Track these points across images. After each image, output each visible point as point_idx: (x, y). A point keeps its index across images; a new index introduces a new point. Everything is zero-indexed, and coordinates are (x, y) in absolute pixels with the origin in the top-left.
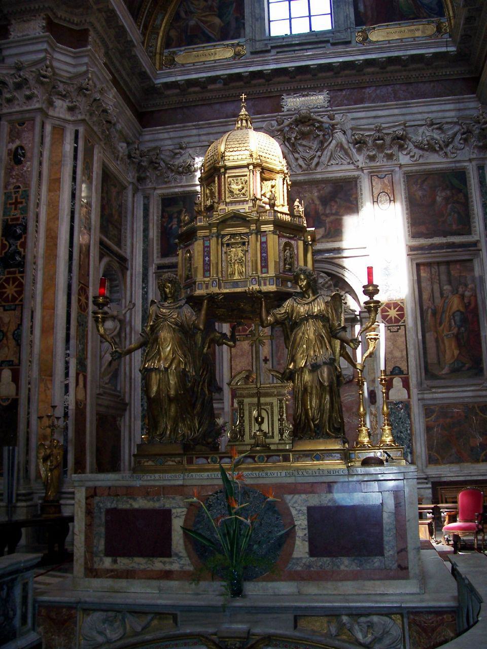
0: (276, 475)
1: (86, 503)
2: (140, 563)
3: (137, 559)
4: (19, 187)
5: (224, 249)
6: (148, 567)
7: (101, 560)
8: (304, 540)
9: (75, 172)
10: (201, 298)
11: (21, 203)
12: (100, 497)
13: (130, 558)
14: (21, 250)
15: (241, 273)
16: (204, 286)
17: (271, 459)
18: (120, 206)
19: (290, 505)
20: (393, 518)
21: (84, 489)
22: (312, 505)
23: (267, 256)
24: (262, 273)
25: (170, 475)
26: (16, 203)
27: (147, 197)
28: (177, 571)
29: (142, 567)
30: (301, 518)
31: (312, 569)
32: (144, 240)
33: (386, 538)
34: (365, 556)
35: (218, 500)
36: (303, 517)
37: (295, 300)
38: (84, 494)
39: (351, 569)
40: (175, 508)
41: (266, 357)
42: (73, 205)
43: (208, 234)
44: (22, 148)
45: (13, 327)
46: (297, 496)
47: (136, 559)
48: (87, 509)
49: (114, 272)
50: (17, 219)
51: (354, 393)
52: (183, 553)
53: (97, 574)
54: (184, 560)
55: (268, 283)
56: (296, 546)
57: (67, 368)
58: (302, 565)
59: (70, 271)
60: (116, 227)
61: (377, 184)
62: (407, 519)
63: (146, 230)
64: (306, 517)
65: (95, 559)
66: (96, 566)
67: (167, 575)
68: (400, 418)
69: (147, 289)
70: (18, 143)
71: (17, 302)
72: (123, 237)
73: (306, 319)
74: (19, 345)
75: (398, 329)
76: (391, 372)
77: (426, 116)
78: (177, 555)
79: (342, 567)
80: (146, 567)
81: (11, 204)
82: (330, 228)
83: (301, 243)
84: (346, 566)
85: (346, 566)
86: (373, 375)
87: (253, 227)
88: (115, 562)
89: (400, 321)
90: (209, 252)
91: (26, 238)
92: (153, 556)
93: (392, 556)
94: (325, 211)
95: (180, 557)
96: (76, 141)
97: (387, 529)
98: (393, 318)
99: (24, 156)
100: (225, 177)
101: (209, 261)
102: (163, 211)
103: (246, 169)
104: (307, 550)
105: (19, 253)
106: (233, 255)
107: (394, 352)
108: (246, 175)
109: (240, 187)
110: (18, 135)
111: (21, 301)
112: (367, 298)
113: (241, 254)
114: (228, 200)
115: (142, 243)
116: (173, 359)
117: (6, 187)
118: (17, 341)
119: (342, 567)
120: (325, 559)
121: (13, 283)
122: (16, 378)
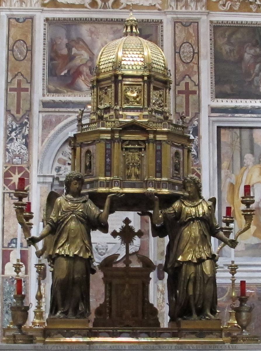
0: (167, 348)
10: (104, 195)
15: (137, 176)
16: (105, 184)
37: (183, 203)
43: (109, 138)
61: (180, 31)
73: (193, 220)
83: (186, 151)
87: (151, 136)
100: (121, 85)
103: (141, 80)
106: (130, 158)
109: (135, 95)
112: (243, 207)
113: (137, 158)
114: (125, 106)
116: (81, 248)
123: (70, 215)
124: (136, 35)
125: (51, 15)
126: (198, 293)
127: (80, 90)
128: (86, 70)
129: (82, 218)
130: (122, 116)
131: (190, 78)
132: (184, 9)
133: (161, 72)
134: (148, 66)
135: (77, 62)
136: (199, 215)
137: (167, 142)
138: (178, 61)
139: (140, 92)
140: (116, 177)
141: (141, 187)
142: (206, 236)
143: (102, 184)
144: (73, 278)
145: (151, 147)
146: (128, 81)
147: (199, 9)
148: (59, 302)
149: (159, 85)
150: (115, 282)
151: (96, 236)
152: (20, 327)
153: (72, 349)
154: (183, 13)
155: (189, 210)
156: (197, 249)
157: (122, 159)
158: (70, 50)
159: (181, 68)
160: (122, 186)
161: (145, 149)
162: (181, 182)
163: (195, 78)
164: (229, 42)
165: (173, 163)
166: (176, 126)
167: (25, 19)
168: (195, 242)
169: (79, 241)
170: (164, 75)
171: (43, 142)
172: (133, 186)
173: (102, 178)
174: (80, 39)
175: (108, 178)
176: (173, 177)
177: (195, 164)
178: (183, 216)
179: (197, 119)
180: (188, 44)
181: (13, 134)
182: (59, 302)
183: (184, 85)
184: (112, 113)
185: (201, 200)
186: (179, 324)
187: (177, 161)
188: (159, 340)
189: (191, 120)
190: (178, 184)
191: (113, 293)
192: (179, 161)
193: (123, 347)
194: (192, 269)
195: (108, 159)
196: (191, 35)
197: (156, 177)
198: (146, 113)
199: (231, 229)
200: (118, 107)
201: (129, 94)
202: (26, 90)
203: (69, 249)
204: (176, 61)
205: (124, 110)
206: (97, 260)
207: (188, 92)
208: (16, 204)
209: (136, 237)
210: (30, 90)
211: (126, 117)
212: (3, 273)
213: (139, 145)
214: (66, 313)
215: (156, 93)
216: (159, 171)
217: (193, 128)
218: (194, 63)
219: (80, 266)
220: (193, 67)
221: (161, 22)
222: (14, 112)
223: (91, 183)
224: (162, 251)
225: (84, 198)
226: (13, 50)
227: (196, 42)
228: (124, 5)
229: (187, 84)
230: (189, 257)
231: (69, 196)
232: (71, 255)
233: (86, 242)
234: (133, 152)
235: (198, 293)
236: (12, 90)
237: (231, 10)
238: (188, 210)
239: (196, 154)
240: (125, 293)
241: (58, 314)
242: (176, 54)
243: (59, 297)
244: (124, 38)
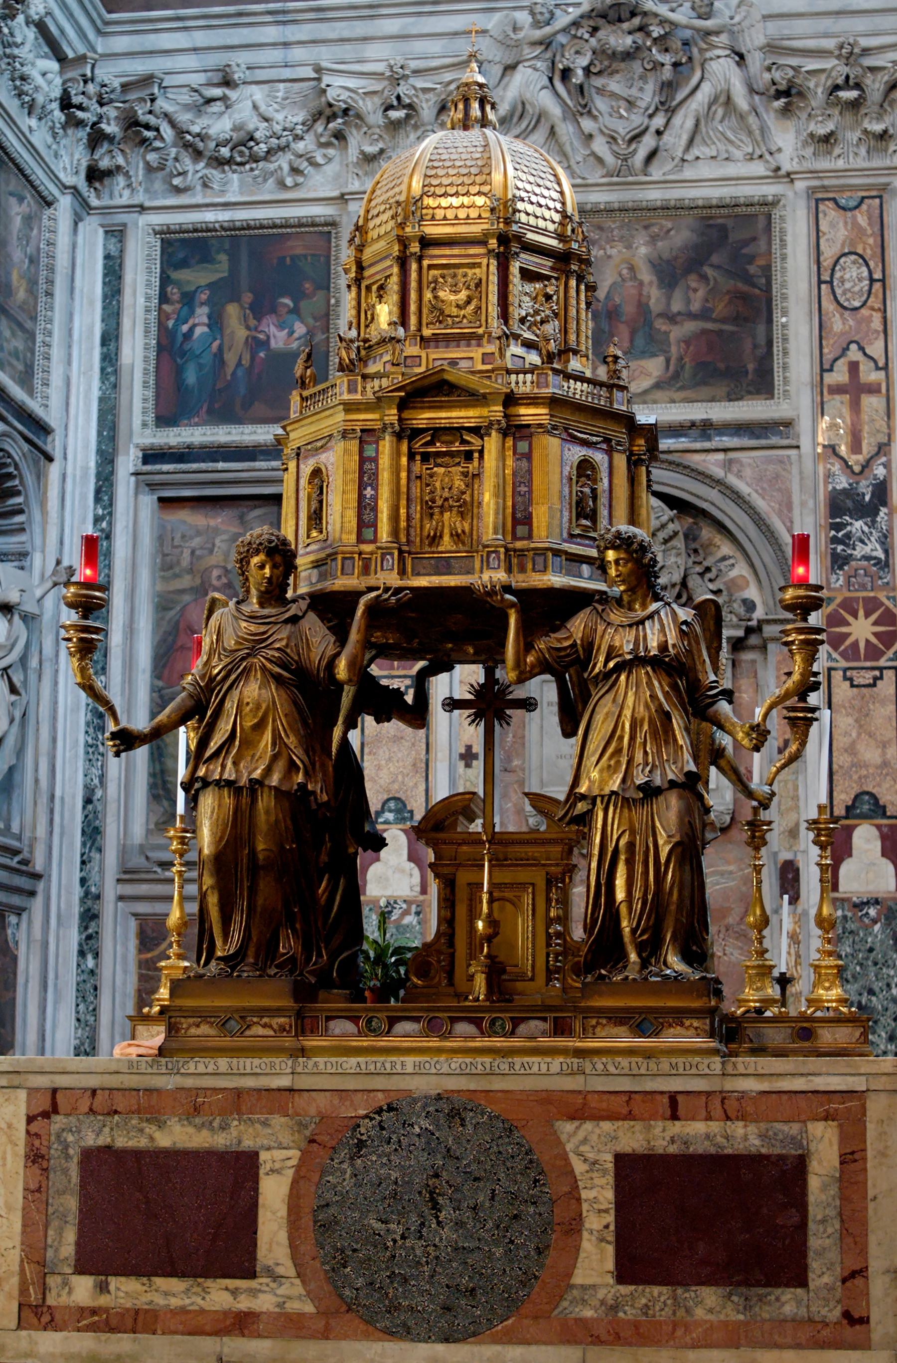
0: (535, 1069)
1: (28, 1132)
5: (417, 467)
6: (192, 1304)
7: (65, 1283)
8: (602, 1240)
10: (353, 596)
12: (67, 1115)
13: (145, 1280)
15: (457, 537)
16: (358, 564)
17: (522, 1028)
18: (33, 261)
19: (569, 1147)
20: (834, 1190)
21: (22, 1095)
22: (628, 1150)
23: (530, 492)
24: (515, 538)
25: (256, 1061)
27: (116, 233)
28: (268, 1313)
29: (175, 1302)
30: (597, 1181)
31: (621, 1314)
32: (103, 370)
33: (814, 1243)
34: (758, 1284)
35: (382, 1128)
36: (603, 1181)
38: (22, 1110)
39: (722, 1317)
40: (269, 1149)
41: (469, 748)
46: (588, 1126)
47: (159, 1281)
48: (30, 1145)
49: (11, 469)
51: (732, 868)
52: (287, 1268)
53: (52, 1320)
54: (288, 1285)
55: (530, 566)
56: (582, 1255)
58: (595, 1302)
60: (20, 326)
61: (832, 225)
62: (871, 1194)
64: (610, 1179)
65: (53, 1281)
66: (51, 1301)
68: (871, 950)
69: (110, 524)
72: (39, 361)
75: (876, 679)
76: (848, 808)
79: (699, 1313)
80: (187, 1301)
82: (681, 359)
83: (621, 461)
84: (711, 1311)
85: (711, 1311)
86: (793, 816)
88: (103, 1288)
89: (883, 653)
90: (376, 474)
92: (206, 1276)
93: (830, 1289)
94: (668, 304)
95: (276, 1278)
97: (819, 1217)
98: (862, 645)
101: (375, 498)
102: (165, 280)
104: (610, 1265)
106: (438, 485)
107: (861, 747)
108: (479, 265)
109: (463, 295)
113: (459, 483)
114: (427, 332)
116: (275, 758)
119: (699, 1313)
120: (656, 1290)
123: (243, 659)
126: (637, 894)
129: (277, 670)
131: (862, 349)
133: (551, 227)
136: (646, 649)
138: (828, 305)
139: (478, 284)
149: (543, 265)
153: (242, 1071)
156: (639, 757)
159: (838, 324)
161: (481, 452)
162: (594, 553)
163: (876, 349)
165: (571, 492)
172: (444, 566)
177: (880, 582)
179: (884, 459)
180: (853, 257)
183: (845, 369)
185: (654, 606)
187: (587, 490)
189: (867, 465)
192: (594, 491)
193: (398, 1067)
195: (369, 489)
196: (861, 230)
197: (515, 538)
199: (814, 710)
203: (235, 764)
204: (824, 303)
213: (464, 442)
215: (529, 288)
217: (873, 485)
218: (873, 309)
220: (869, 319)
224: (791, 824)
227: (878, 250)
229: (854, 367)
234: (446, 466)
239: (882, 556)
242: (823, 286)
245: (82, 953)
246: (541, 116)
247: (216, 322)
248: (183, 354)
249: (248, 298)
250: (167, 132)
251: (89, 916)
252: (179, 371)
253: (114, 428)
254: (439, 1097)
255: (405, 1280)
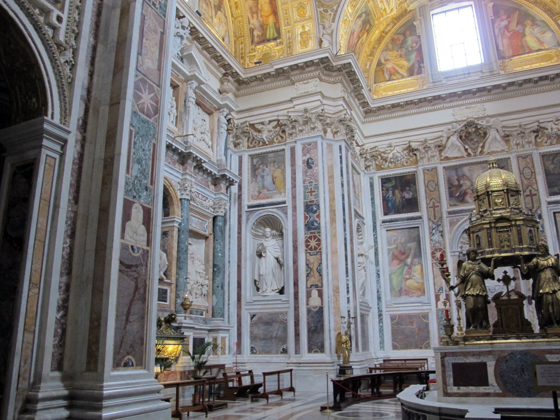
2: (472, 389)
3: (471, 387)
4: (312, 182)
7: (451, 388)
9: (342, 171)
10: (490, 259)
11: (314, 192)
14: (317, 219)
15: (508, 246)
21: (439, 354)
26: (311, 192)
29: (474, 391)
42: (343, 191)
44: (311, 159)
45: (315, 266)
50: (313, 201)
52: (496, 385)
57: (348, 288)
59: (345, 230)
63: (373, 199)
65: (448, 388)
66: (449, 391)
67: (487, 395)
70: (308, 156)
71: (318, 250)
74: (321, 275)
77: (553, 115)
78: (492, 385)
81: (308, 192)
83: (536, 229)
88: (459, 389)
91: (319, 212)
95: (493, 386)
96: (341, 152)
99: (313, 163)
102: (382, 186)
105: (316, 222)
109: (500, 201)
110: (308, 152)
111: (320, 249)
113: (507, 236)
115: (371, 207)
117: (304, 182)
118: (319, 273)
121: (314, 239)
122: (320, 294)
124: (496, 168)
125: (446, 165)
127: (467, 202)
128: (469, 191)
130: (494, 214)
132: (522, 149)
134: (506, 184)
135: (464, 188)
137: (523, 225)
140: (495, 248)
141: (511, 252)
142: (556, 277)
143: (488, 253)
144: (478, 307)
145: (514, 229)
146: (495, 194)
147: (531, 148)
148: (471, 321)
149: (514, 193)
150: (503, 308)
151: (488, 282)
152: (450, 336)
154: (522, 151)
155: (543, 262)
156: (551, 285)
157: (498, 238)
158: (459, 181)
159: (525, 182)
160: (500, 252)
161: (511, 230)
162: (535, 247)
163: (535, 186)
164: (553, 163)
166: (527, 215)
167: (432, 169)
168: (549, 281)
169: (478, 286)
170: (516, 188)
171: (451, 233)
172: (506, 252)
173: (488, 249)
174: (464, 175)
175: (491, 249)
176: (530, 244)
178: (540, 266)
181: (434, 231)
182: (471, 321)
184: (488, 213)
186: (546, 330)
188: (535, 340)
189: (536, 211)
190: (534, 249)
191: (503, 314)
194: (550, 297)
196: (528, 163)
198: (508, 210)
200: (491, 209)
201: (497, 201)
202: (438, 206)
203: (473, 290)
205: (495, 210)
206: (490, 296)
207: (531, 195)
208: (440, 269)
209: (512, 281)
210: (440, 207)
211: (497, 214)
212: (437, 307)
214: (475, 327)
216: (521, 242)
219: (480, 300)
221: (509, 158)
222: (432, 219)
223: (481, 253)
225: (479, 262)
226: (428, 187)
228: (486, 153)
229: (530, 191)
230: (547, 290)
231: (470, 261)
232: (475, 294)
233: (483, 286)
235: (555, 311)
236: (430, 207)
237: (551, 144)
238: (542, 262)
240: (509, 314)
241: (471, 328)
243: (471, 319)
244: (489, 171)
245: (379, 323)
246: (457, 146)
247: (394, 194)
248: (388, 200)
249: (400, 188)
250: (379, 157)
251: (380, 315)
252: (387, 204)
253: (375, 217)
254: (521, 351)
255: (519, 386)
